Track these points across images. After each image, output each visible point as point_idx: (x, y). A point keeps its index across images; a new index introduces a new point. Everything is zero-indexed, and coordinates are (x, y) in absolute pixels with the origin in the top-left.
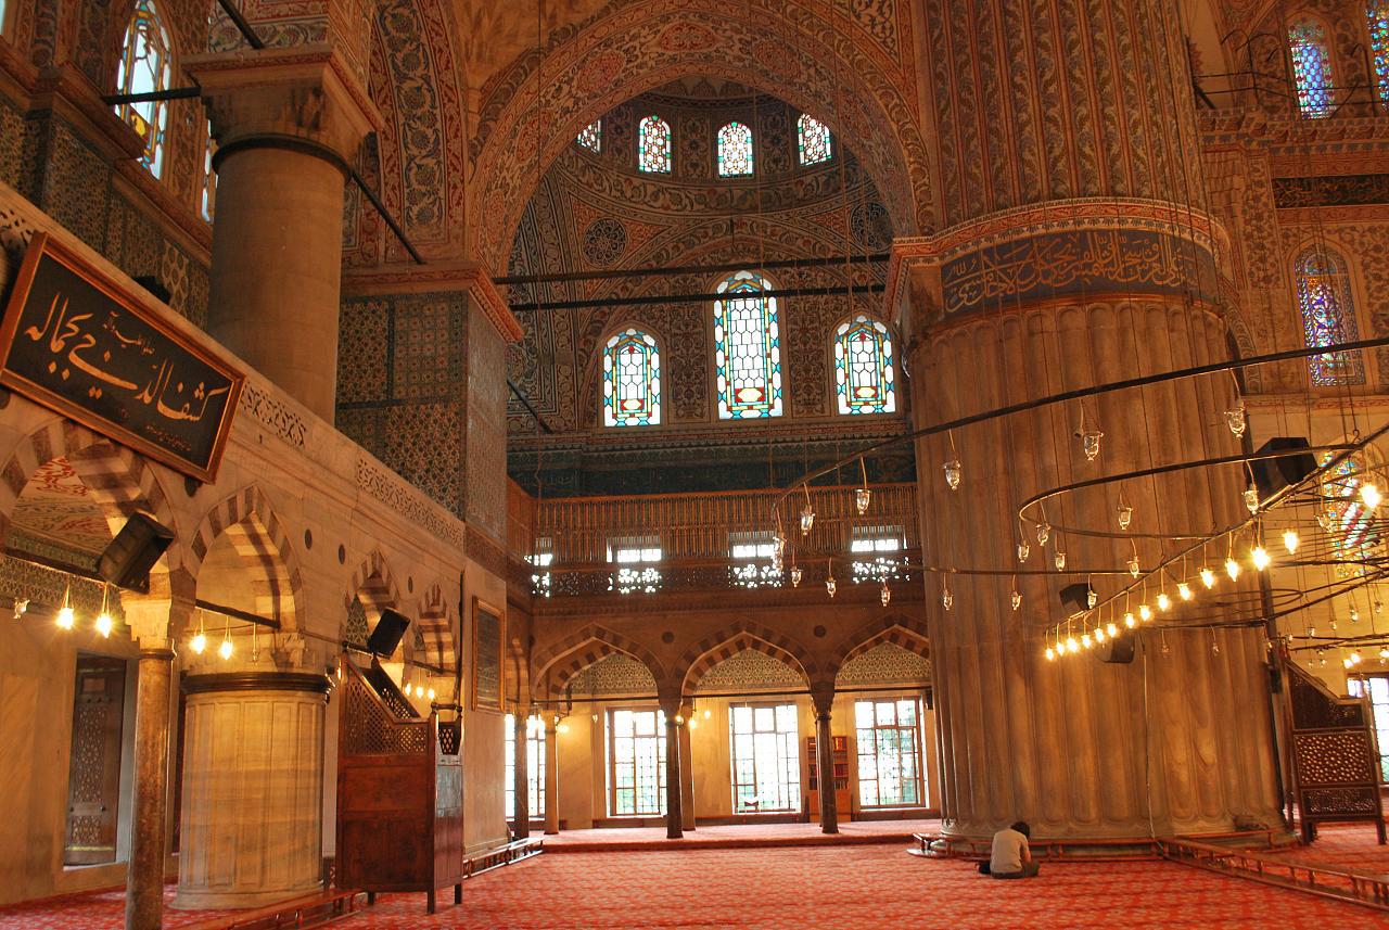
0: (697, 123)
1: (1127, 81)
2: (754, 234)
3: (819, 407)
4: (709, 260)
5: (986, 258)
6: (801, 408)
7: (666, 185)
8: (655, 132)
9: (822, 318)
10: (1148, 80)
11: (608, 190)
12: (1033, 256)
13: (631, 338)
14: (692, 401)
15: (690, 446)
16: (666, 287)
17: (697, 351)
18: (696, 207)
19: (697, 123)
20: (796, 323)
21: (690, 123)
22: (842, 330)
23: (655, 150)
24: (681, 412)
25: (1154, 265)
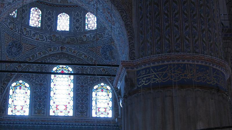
0: (51, 12)
1: (201, 16)
2: (68, 52)
3: (85, 114)
4: (51, 59)
5: (152, 70)
6: (79, 114)
7: (38, 32)
8: (36, 13)
9: (89, 83)
10: (208, 16)
11: (18, 31)
12: (168, 70)
13: (20, 84)
14: (41, 108)
15: (38, 124)
16: (35, 67)
17: (44, 91)
18: (48, 40)
19: (51, 12)
20: (79, 84)
21: (48, 11)
22: (95, 87)
23: (36, 19)
24: (36, 112)
25: (207, 77)
